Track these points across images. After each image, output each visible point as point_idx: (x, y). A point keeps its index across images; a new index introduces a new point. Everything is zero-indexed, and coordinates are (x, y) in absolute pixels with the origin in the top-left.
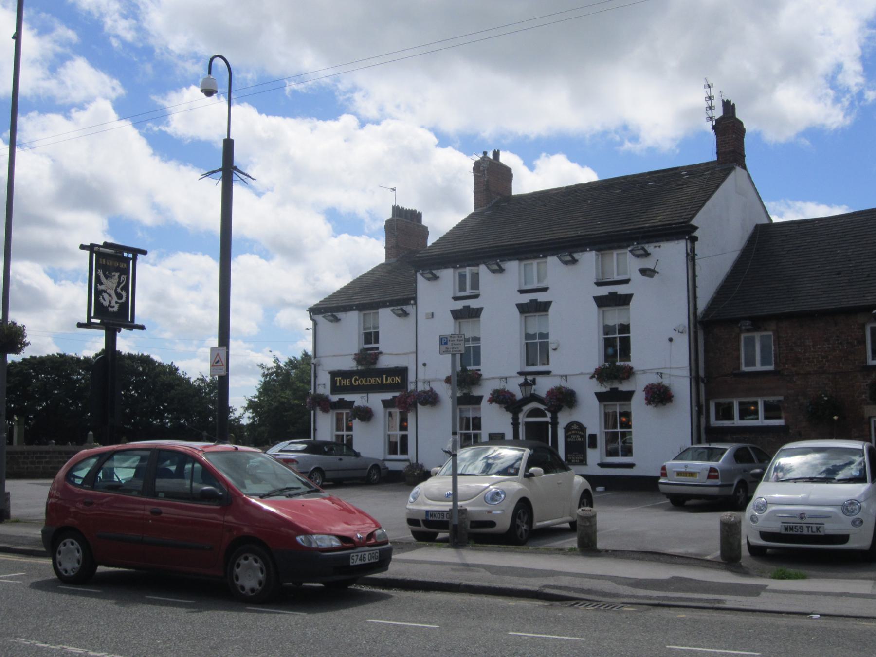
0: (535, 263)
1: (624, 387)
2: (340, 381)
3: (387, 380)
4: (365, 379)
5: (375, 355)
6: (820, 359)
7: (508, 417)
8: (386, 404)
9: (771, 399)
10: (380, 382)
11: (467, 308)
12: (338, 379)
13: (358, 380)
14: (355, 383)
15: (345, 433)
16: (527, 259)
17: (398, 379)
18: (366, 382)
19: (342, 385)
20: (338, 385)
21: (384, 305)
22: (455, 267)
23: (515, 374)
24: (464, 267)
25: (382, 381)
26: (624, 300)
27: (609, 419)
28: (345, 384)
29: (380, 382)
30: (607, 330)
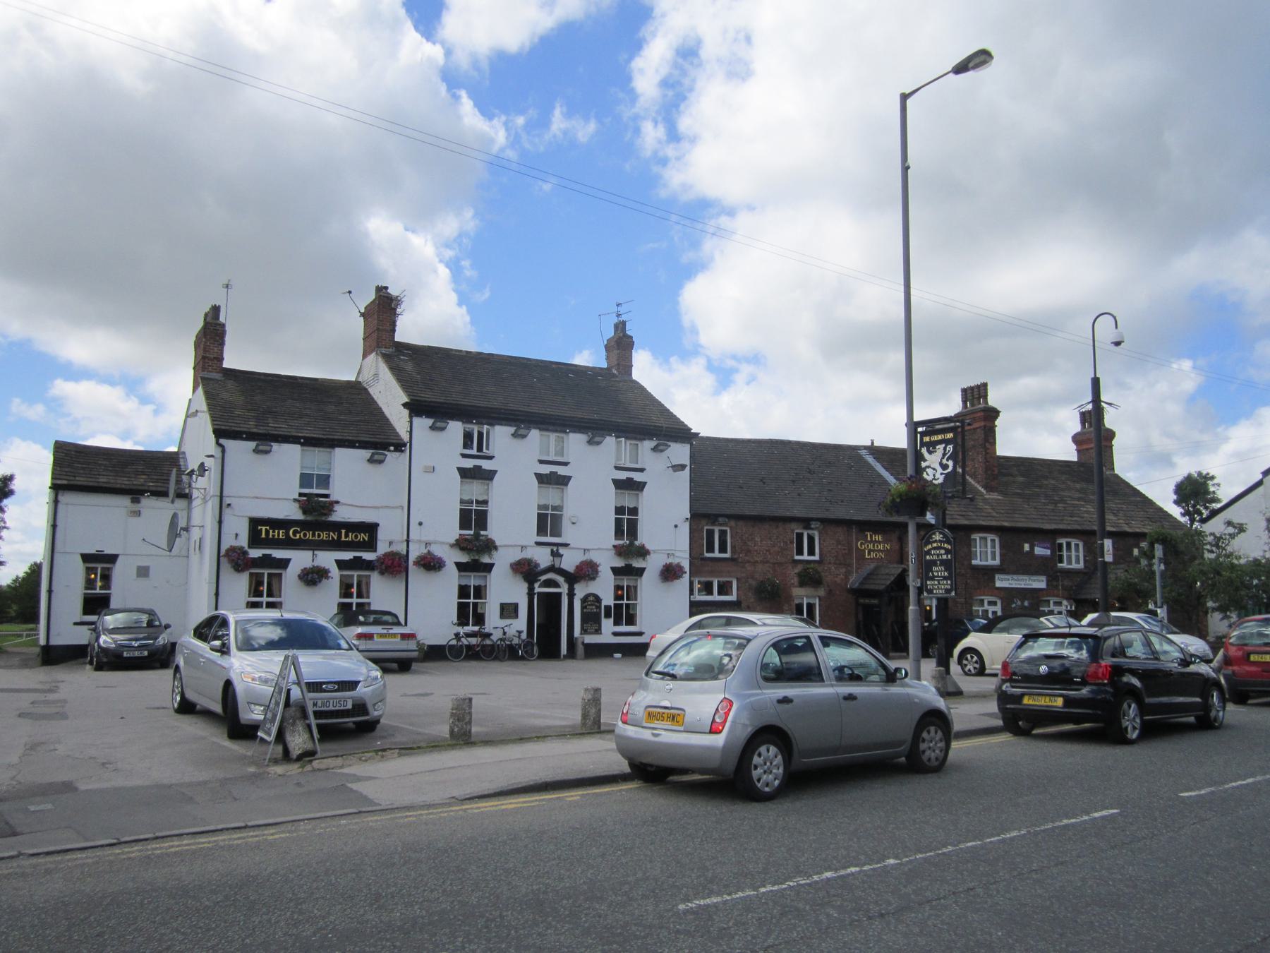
0: (553, 437)
1: (637, 563)
2: (267, 532)
3: (347, 536)
4: (311, 532)
5: (329, 507)
6: (765, 552)
7: (524, 587)
8: (341, 564)
9: (721, 579)
10: (335, 538)
11: (478, 468)
12: (264, 528)
13: (300, 533)
14: (294, 535)
15: (354, 600)
16: (547, 430)
17: (364, 537)
18: (313, 535)
19: (271, 536)
20: (263, 536)
21: (350, 444)
22: (463, 422)
23: (533, 544)
24: (483, 424)
25: (340, 536)
26: (563, 481)
27: (618, 591)
28: (276, 537)
29: (335, 538)
30: (619, 510)
